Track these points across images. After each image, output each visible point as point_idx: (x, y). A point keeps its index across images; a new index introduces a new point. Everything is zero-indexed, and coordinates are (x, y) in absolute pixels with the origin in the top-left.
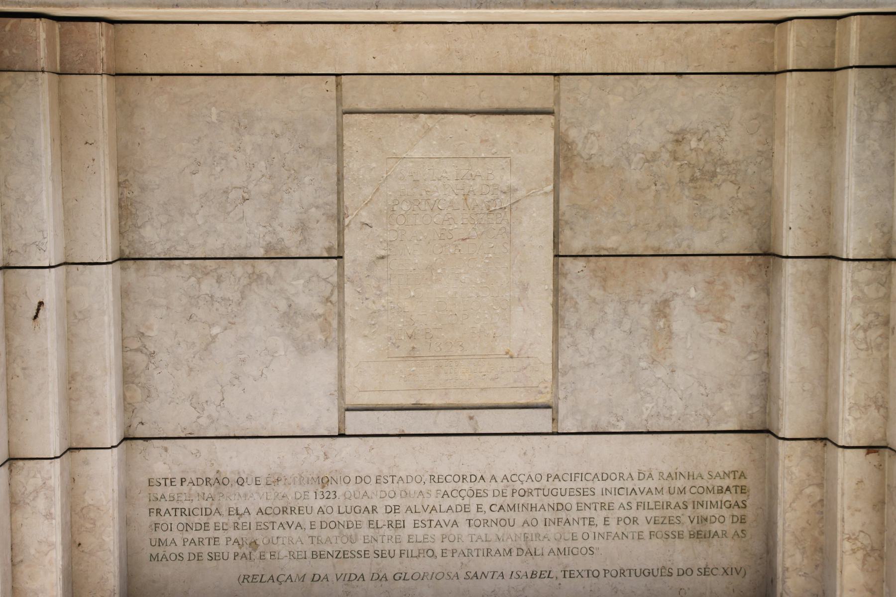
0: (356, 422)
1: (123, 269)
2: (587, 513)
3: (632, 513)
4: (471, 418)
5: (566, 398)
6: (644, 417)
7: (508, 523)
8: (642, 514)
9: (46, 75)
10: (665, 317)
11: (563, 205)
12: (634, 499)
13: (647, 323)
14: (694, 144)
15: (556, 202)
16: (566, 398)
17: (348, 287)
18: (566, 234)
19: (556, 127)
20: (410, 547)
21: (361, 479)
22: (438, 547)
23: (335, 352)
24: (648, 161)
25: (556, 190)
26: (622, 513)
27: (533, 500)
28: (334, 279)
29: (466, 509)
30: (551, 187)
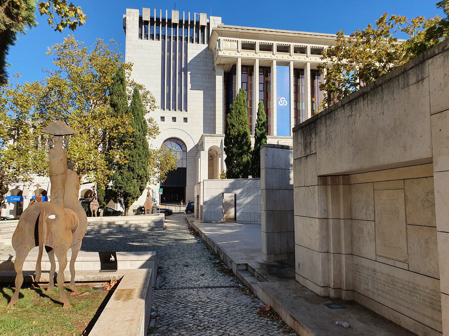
0: (379, 259)
1: (351, 221)
2: (415, 295)
3: (425, 298)
4: (394, 262)
5: (410, 261)
6: (425, 271)
7: (402, 292)
8: (427, 299)
9: (330, 186)
10: (428, 244)
11: (407, 211)
12: (425, 294)
13: (424, 244)
14: (430, 196)
15: (406, 211)
16: (410, 261)
17: (376, 227)
18: (408, 219)
19: (405, 192)
20: (387, 291)
21: (379, 272)
22: (391, 293)
23: (375, 242)
24: (422, 201)
25: (405, 207)
26: (423, 298)
27: (405, 287)
28: (374, 226)
29: (394, 285)
30: (404, 207)
